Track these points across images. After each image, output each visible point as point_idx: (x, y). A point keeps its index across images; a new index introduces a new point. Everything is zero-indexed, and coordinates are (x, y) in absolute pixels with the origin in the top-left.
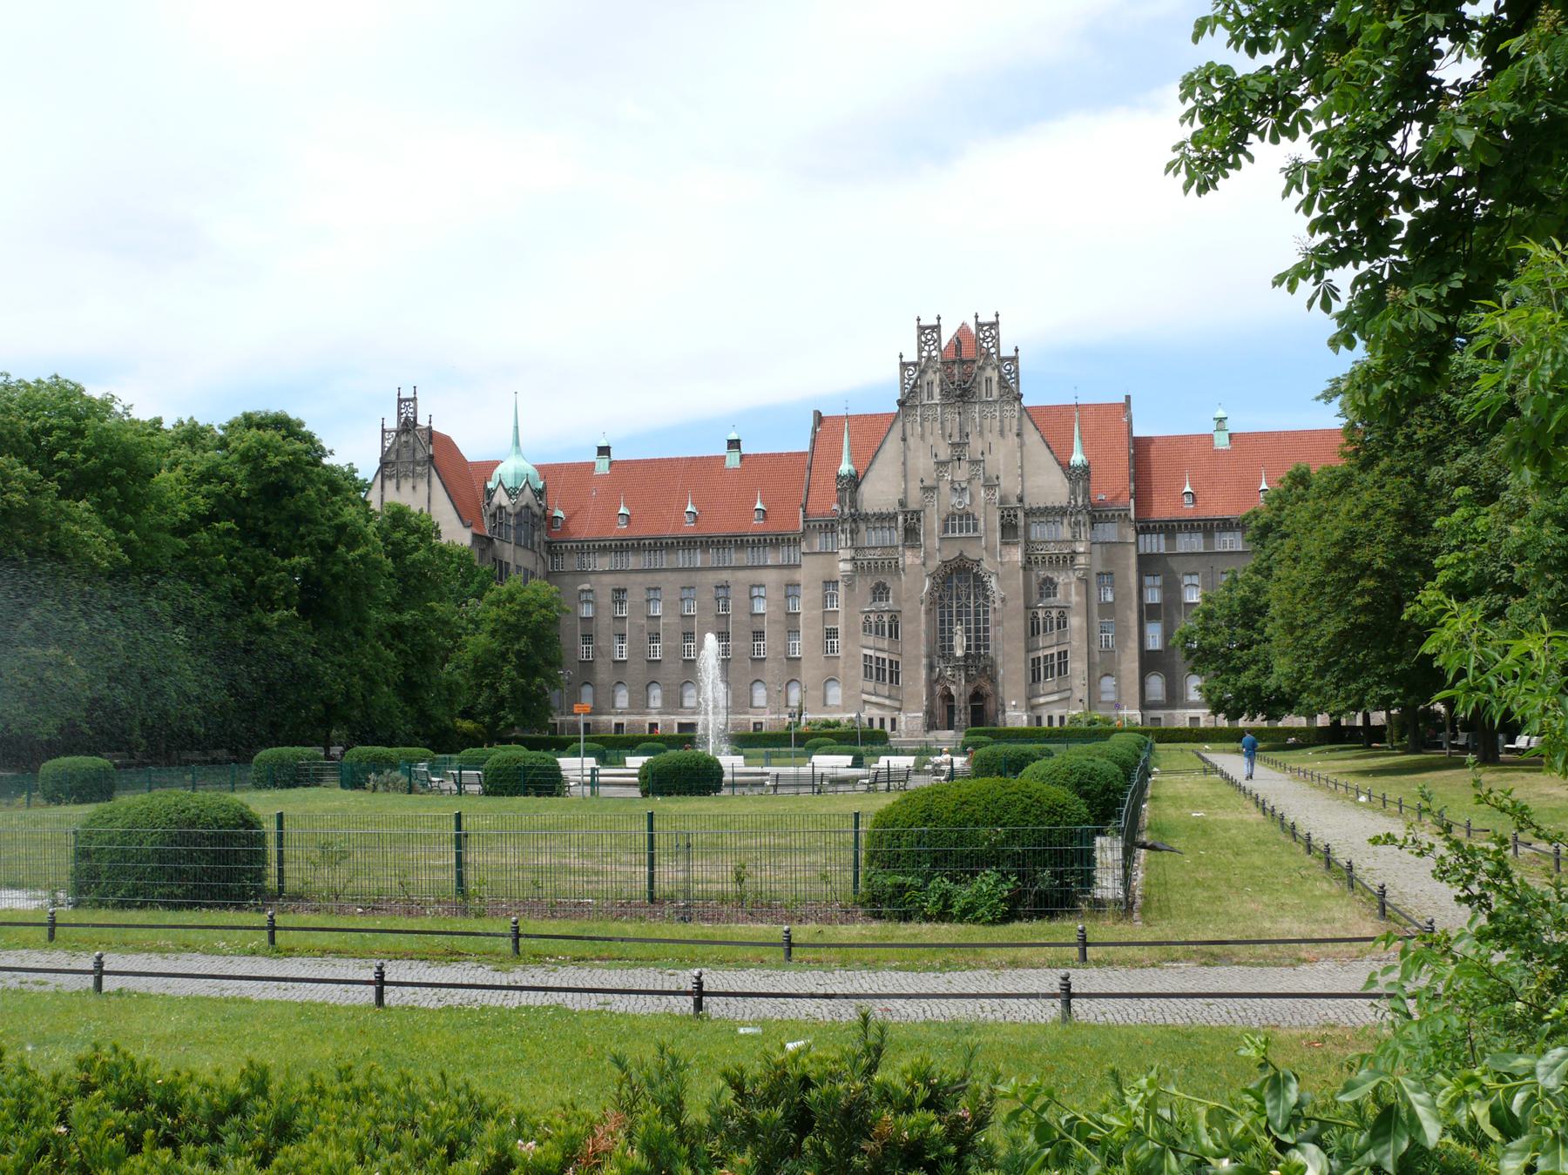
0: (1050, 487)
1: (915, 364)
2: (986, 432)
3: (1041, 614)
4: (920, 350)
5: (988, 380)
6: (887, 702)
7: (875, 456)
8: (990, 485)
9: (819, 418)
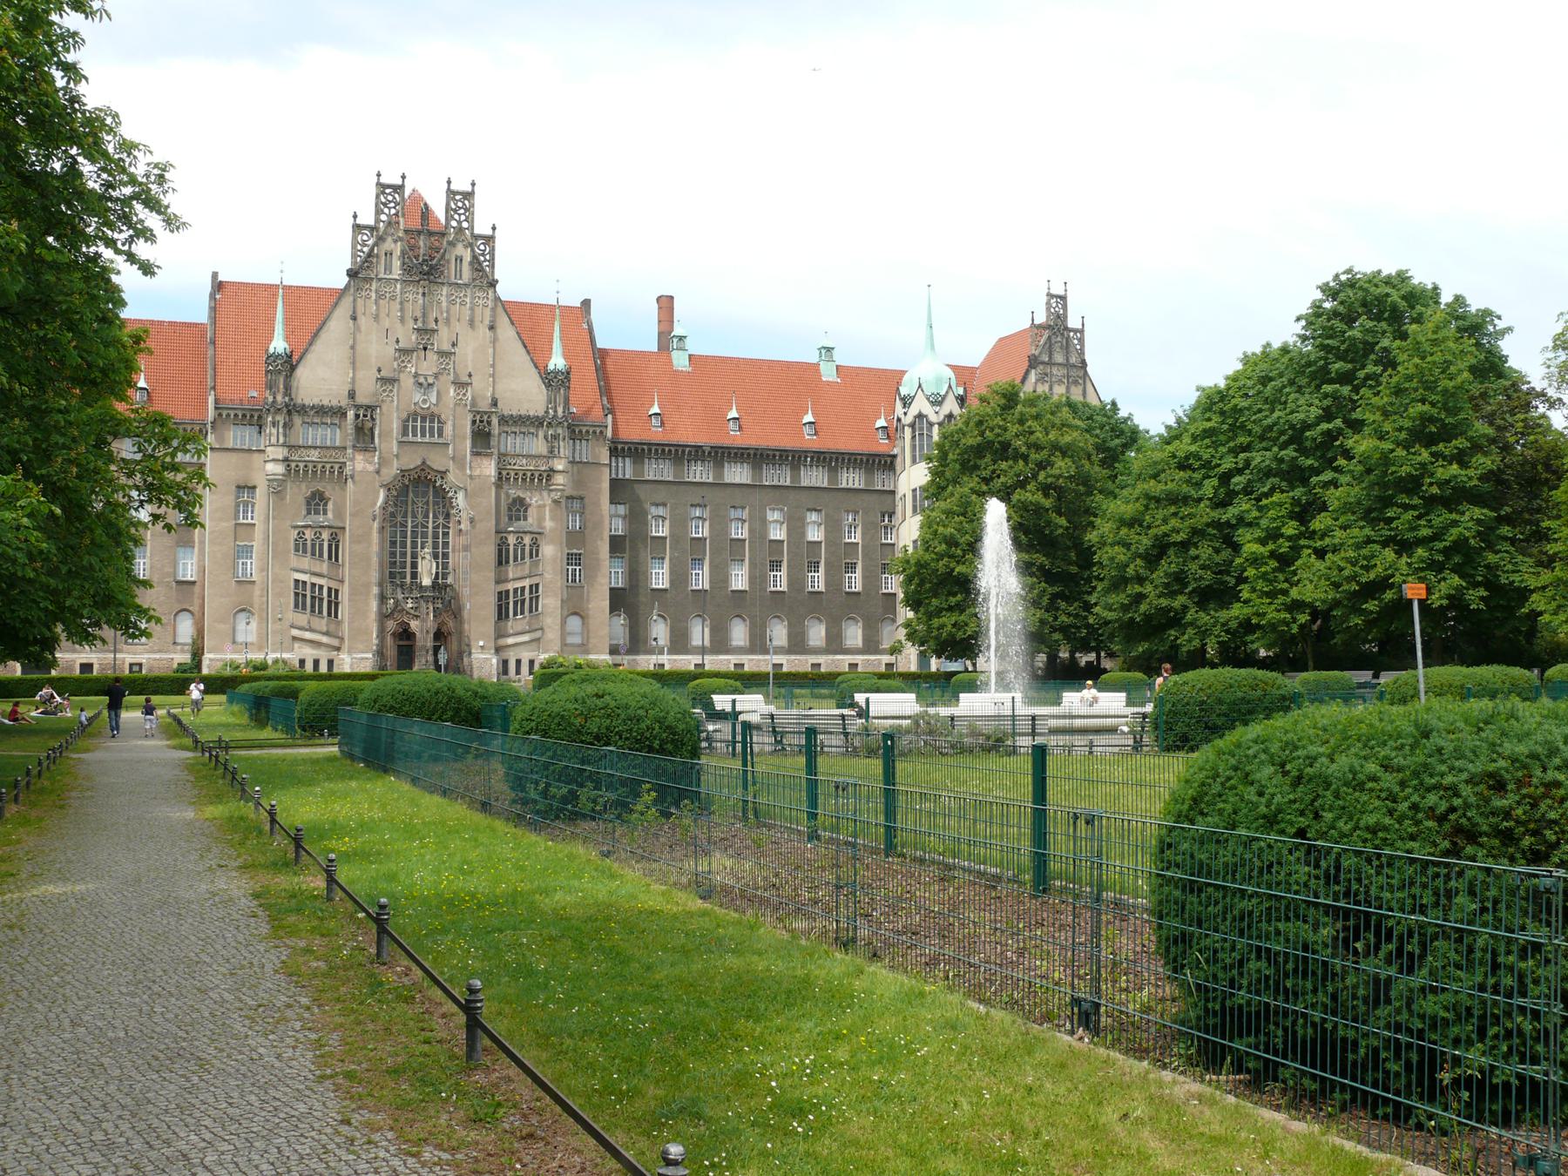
0: (524, 392)
1: (372, 229)
2: (453, 320)
3: (512, 540)
4: (378, 212)
5: (460, 259)
6: (325, 639)
7: (316, 335)
8: (460, 385)
9: (218, 286)
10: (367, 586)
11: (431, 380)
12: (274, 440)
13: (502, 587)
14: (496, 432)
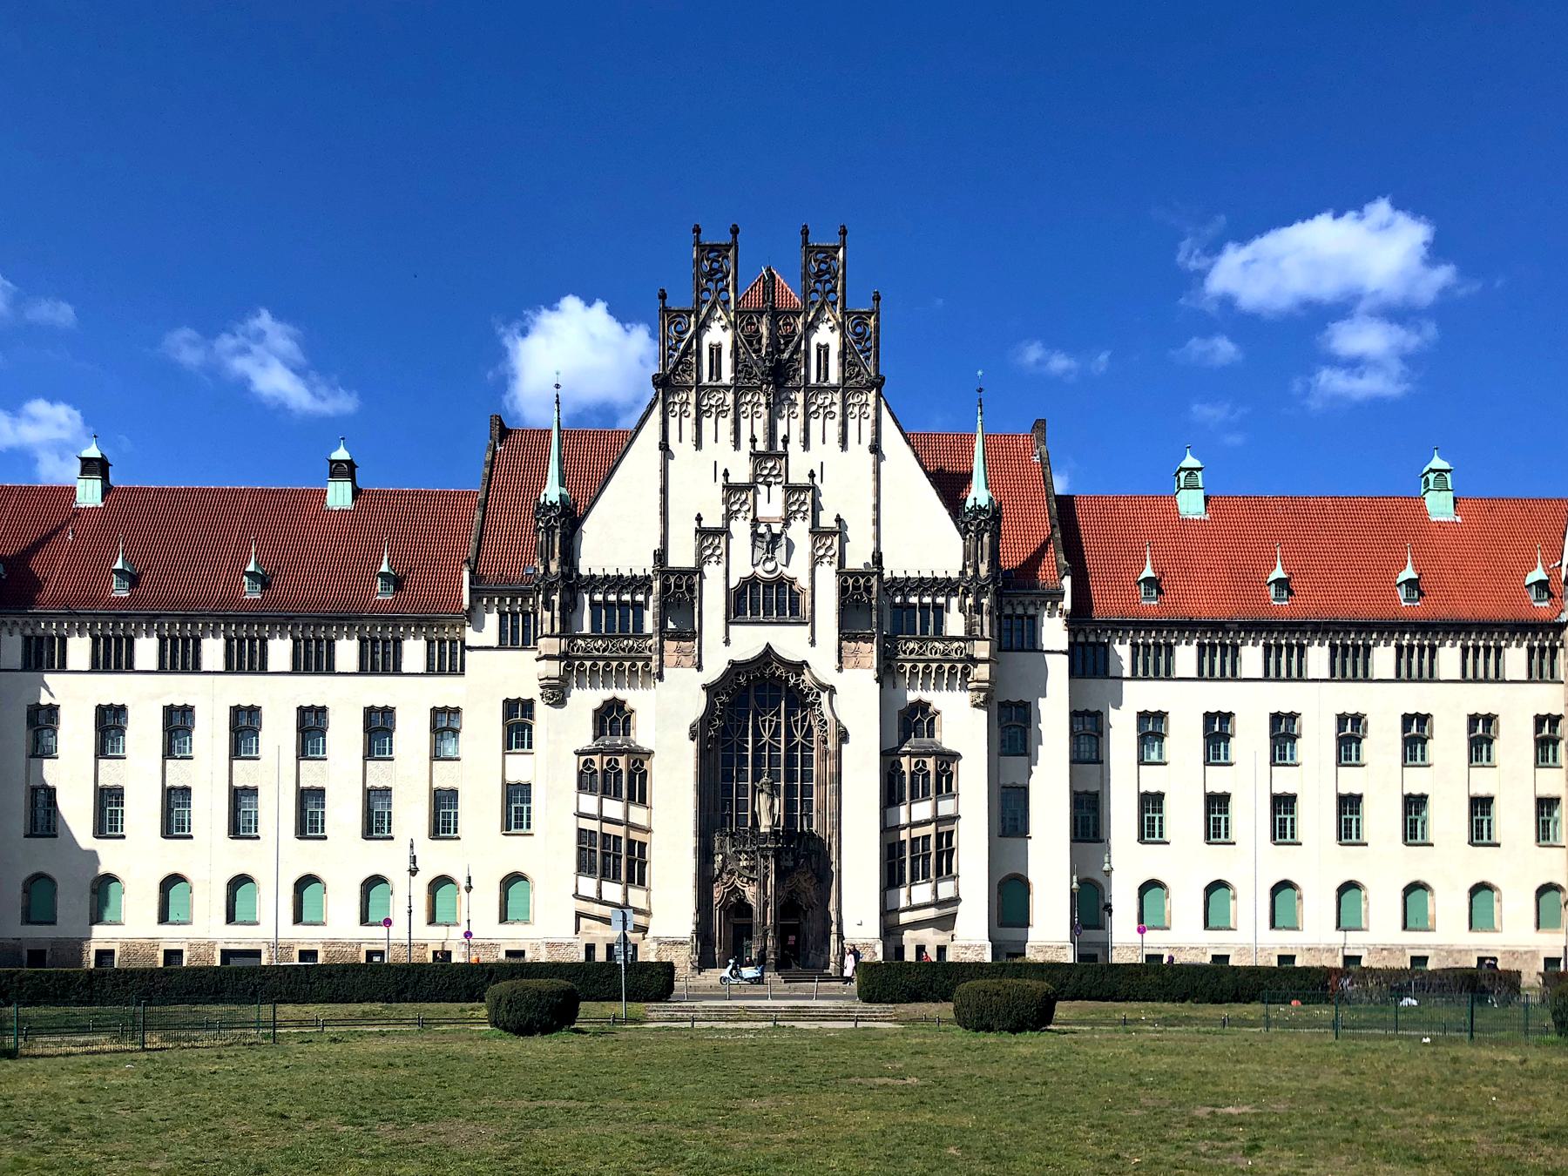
5: (824, 350)
11: (776, 529)
12: (547, 630)
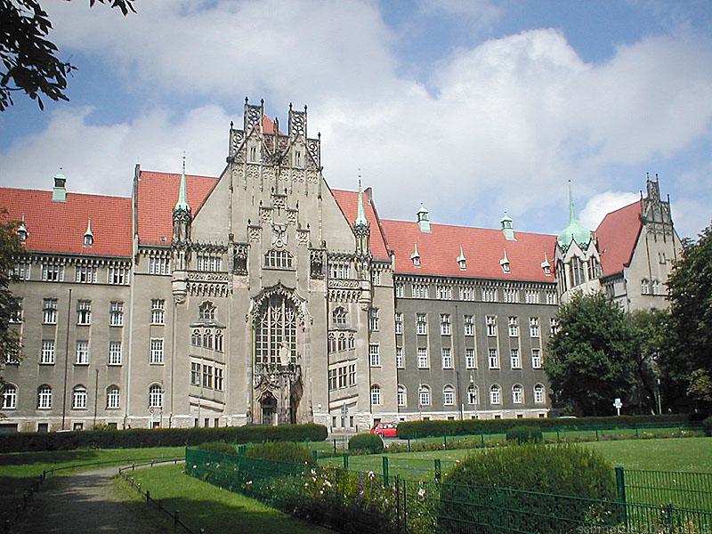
6: (213, 404)
10: (242, 367)
13: (331, 368)
14: (325, 263)
